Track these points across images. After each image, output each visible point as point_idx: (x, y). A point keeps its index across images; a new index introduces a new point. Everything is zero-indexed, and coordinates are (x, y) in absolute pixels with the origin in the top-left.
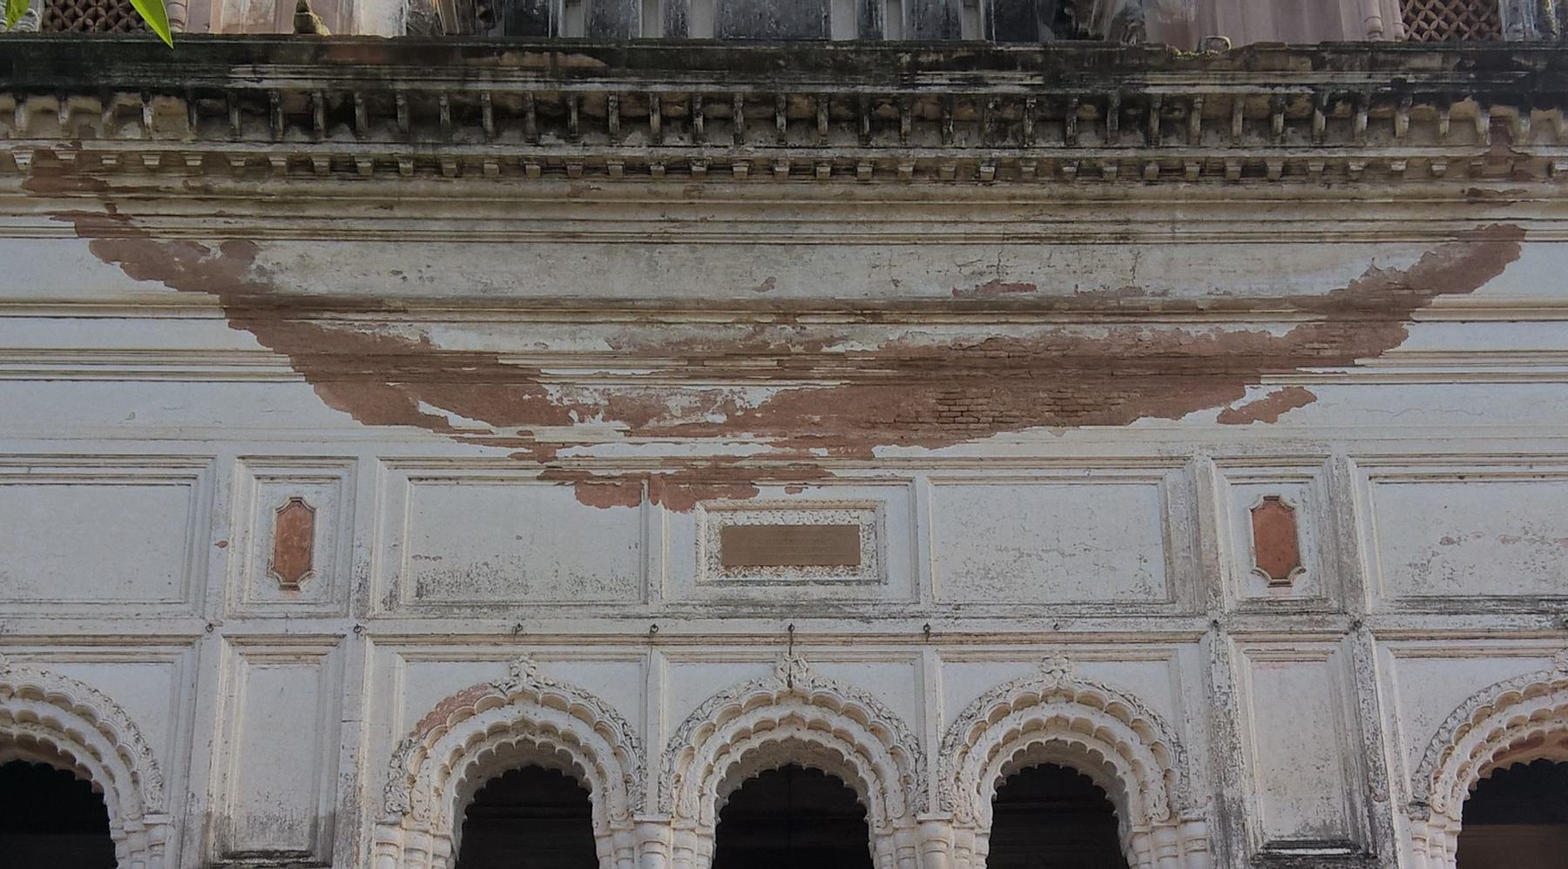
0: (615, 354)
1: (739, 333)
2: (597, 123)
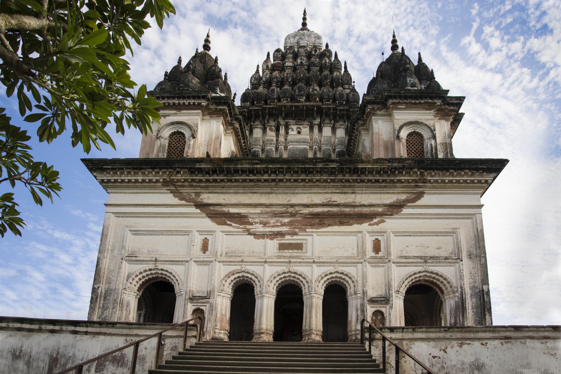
1: (283, 209)
2: (259, 172)
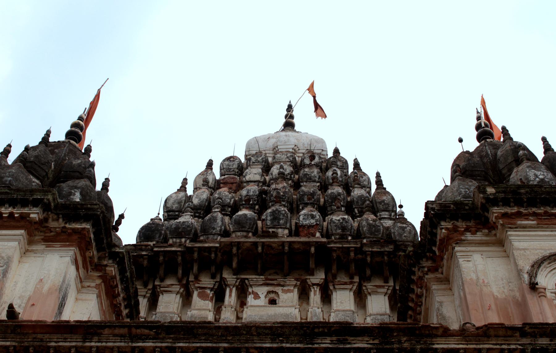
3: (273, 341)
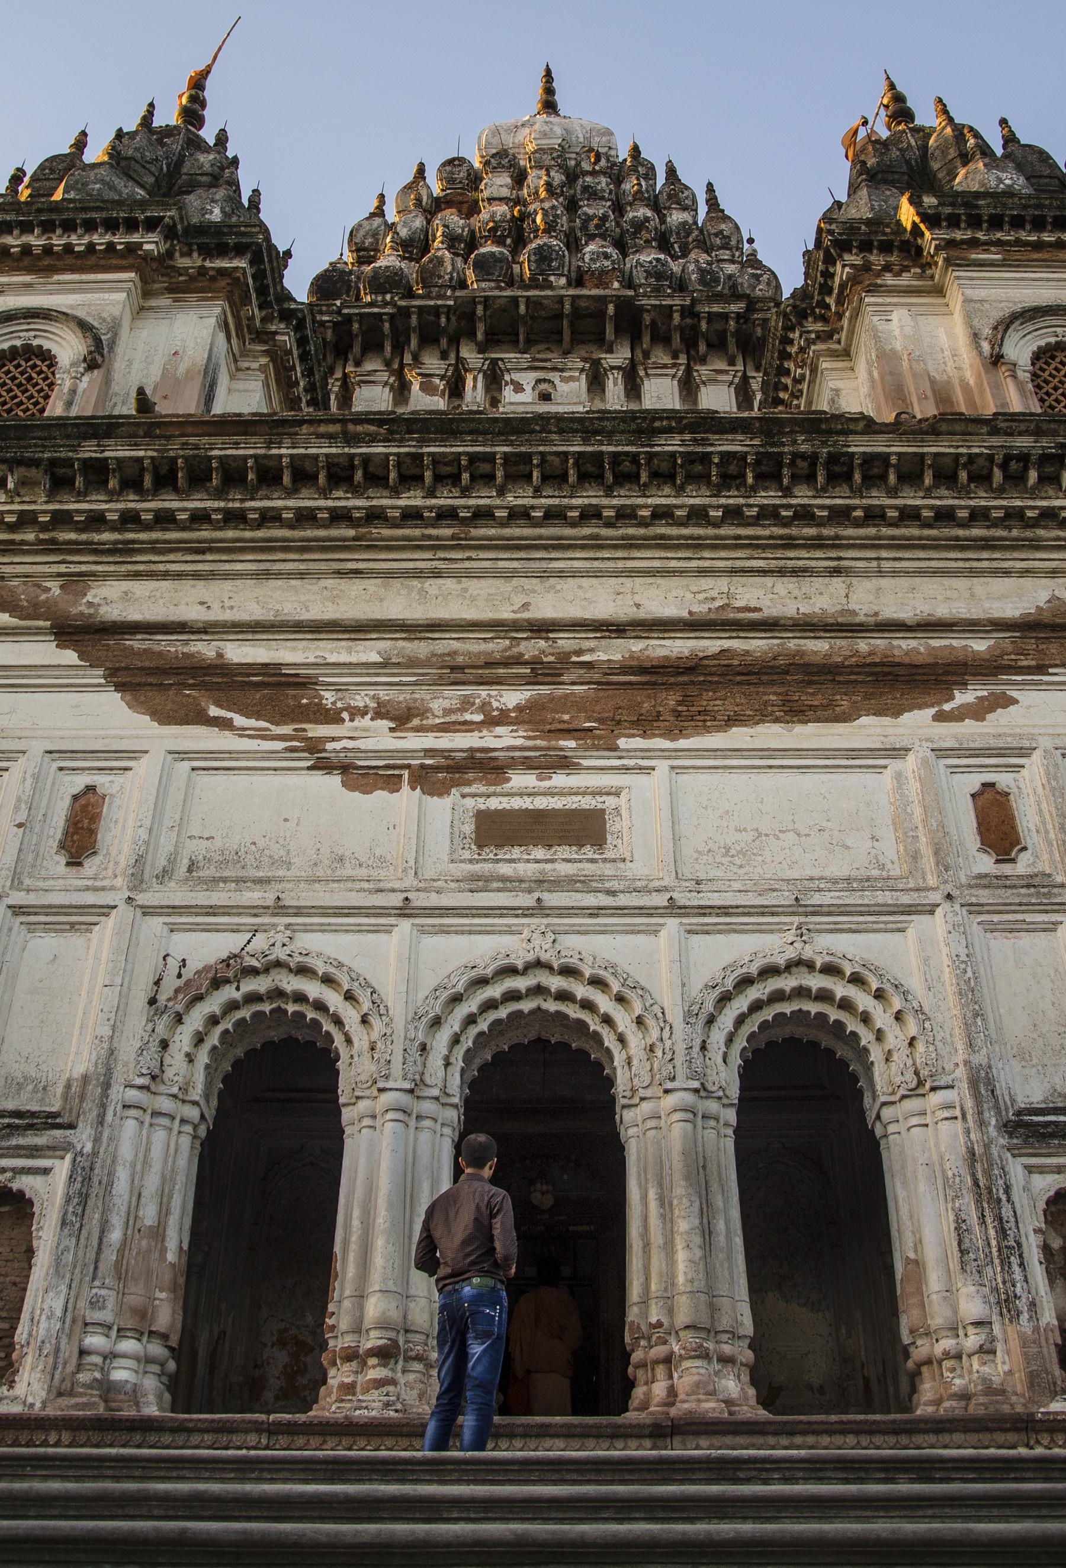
0: (384, 665)
1: (497, 646)
2: (375, 476)
3: (586, 441)
